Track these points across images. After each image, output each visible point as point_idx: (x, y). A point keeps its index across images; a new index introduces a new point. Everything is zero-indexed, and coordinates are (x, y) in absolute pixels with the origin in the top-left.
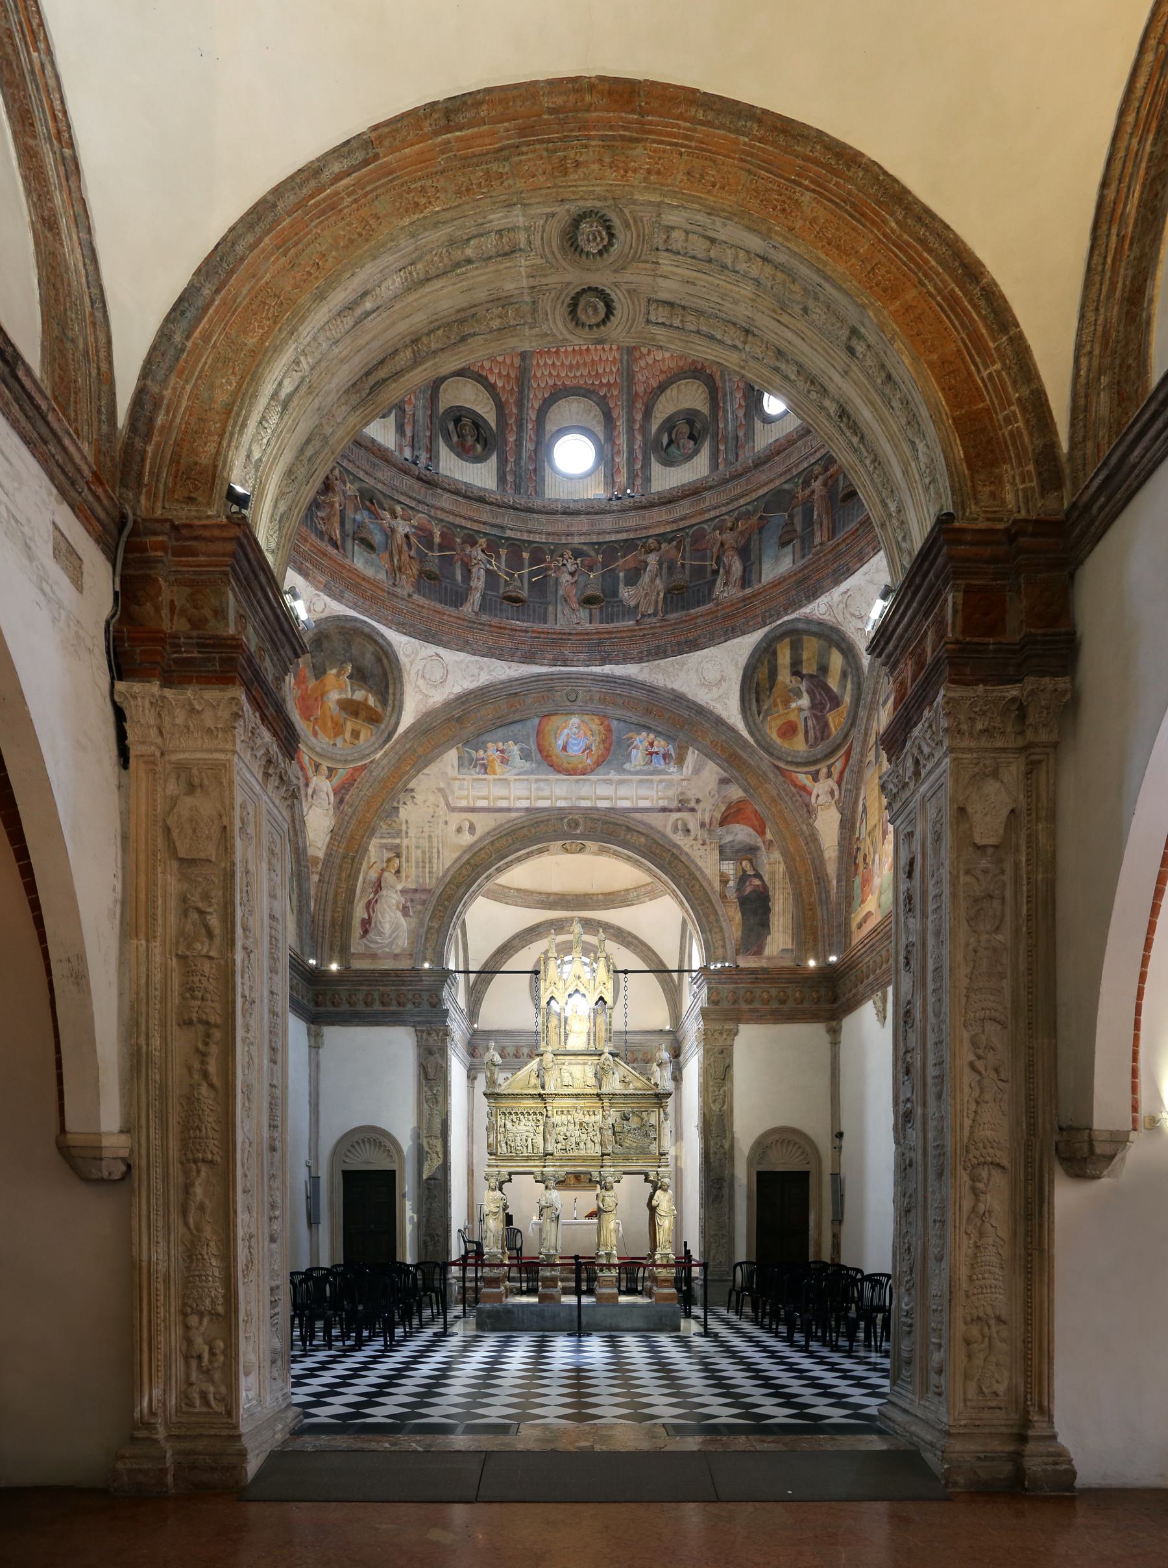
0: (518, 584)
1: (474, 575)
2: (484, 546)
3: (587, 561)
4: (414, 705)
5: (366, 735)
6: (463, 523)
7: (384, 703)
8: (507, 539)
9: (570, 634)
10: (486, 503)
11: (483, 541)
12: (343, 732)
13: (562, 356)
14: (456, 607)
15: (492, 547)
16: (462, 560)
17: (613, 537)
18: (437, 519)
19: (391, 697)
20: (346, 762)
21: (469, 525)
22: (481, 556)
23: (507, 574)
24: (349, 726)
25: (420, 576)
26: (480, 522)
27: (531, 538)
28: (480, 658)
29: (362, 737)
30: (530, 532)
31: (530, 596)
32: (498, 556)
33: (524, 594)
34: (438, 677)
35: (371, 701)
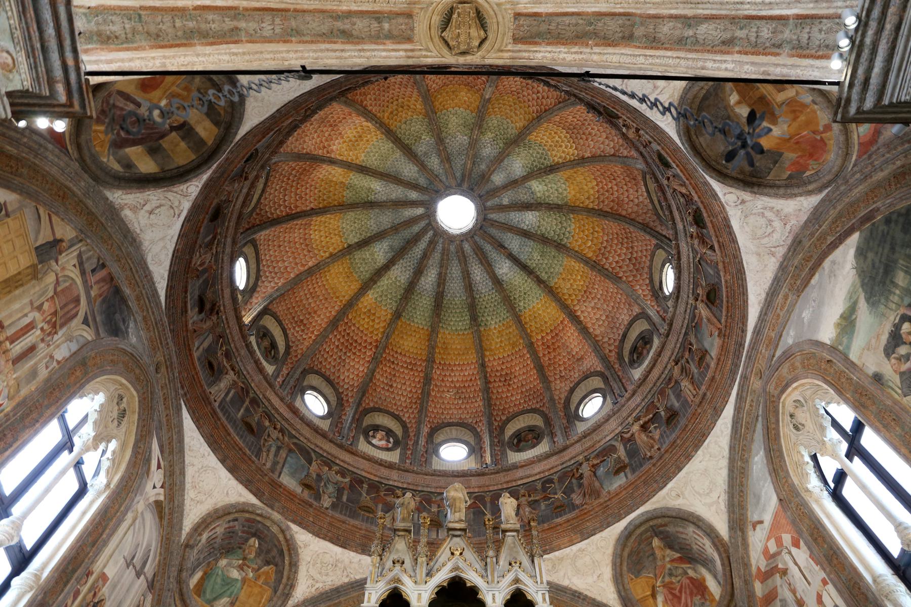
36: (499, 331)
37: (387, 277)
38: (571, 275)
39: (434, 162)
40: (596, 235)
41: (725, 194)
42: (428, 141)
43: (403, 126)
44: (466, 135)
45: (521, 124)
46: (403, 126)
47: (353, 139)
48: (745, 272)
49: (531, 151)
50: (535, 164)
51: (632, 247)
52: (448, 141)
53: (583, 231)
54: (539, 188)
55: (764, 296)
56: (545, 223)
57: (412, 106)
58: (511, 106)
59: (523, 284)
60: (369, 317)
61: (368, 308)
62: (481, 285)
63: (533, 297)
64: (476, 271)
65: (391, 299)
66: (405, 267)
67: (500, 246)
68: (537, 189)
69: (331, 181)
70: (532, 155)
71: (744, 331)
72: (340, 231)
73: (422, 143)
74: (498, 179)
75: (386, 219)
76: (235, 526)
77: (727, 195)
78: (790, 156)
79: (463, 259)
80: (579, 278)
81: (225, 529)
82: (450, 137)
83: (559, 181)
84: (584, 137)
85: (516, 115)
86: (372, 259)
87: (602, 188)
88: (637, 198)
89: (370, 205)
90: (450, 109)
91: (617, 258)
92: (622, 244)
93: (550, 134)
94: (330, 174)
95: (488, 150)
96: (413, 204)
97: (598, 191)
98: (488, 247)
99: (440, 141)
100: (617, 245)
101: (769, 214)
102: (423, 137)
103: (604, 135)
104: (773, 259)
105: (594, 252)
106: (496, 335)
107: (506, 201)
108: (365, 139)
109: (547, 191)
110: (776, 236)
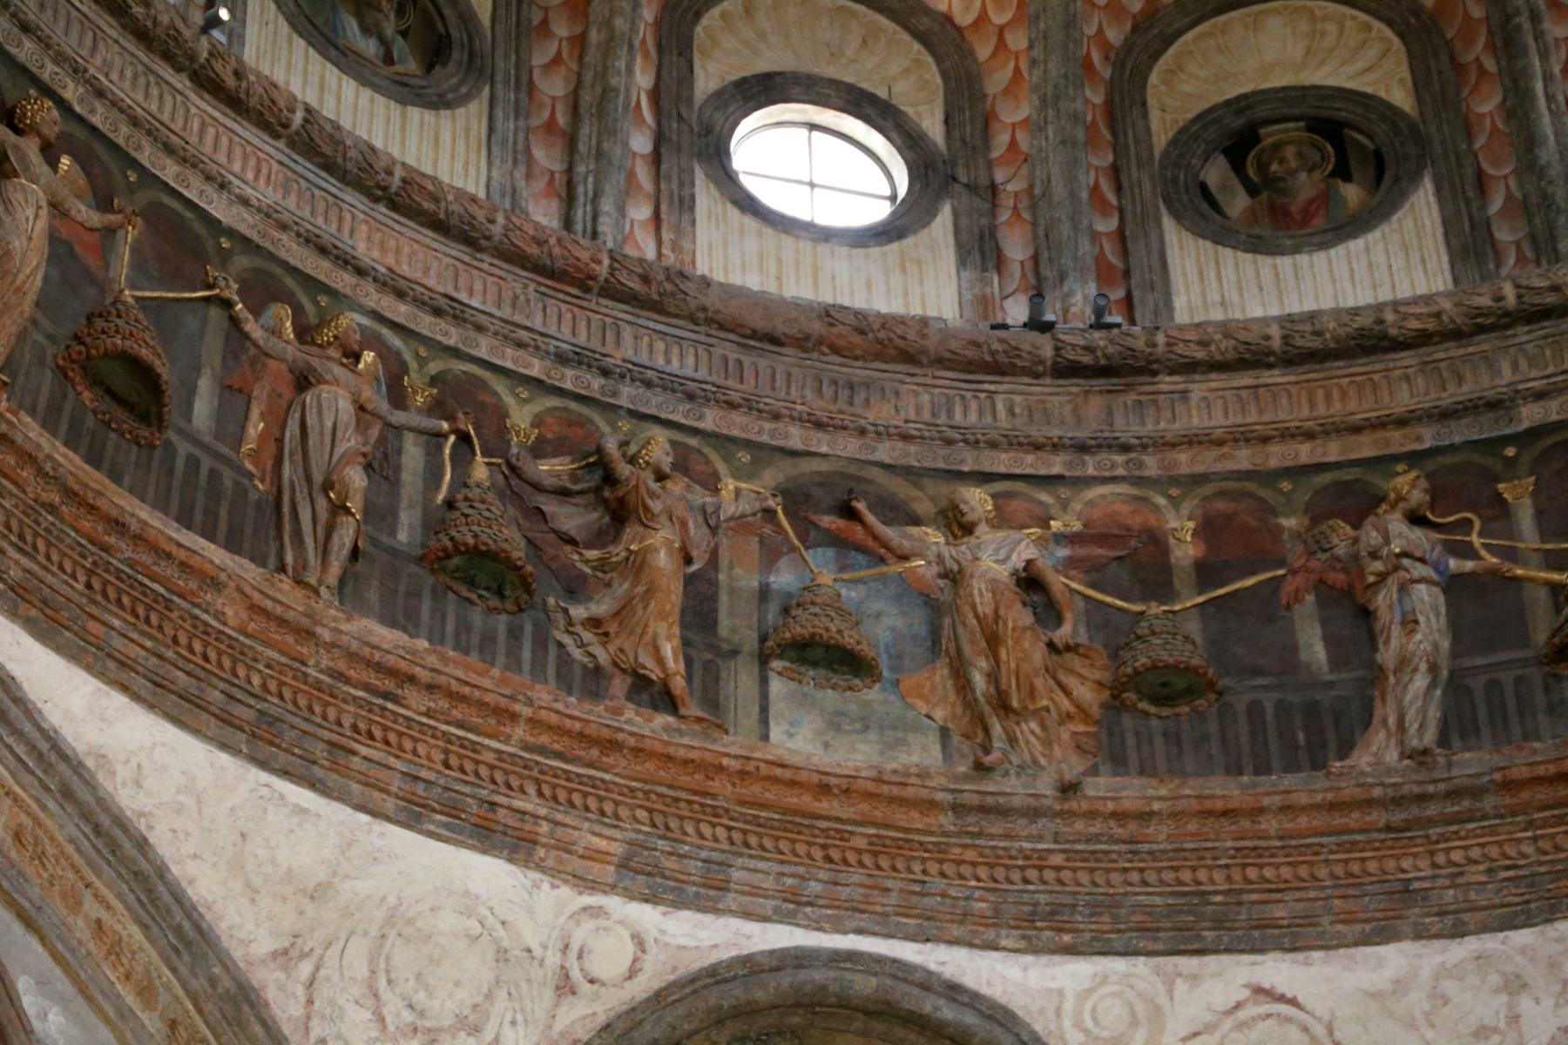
1: (1384, 616)
2: (1418, 496)
6: (1304, 453)
8: (1535, 433)
10: (1398, 345)
11: (1409, 485)
14: (1318, 764)
16: (1321, 586)
18: (1175, 480)
21: (1333, 451)
22: (1402, 535)
25: (1116, 702)
26: (1380, 424)
28: (1490, 943)
32: (1499, 511)
41: (640, 942)
48: (263, 765)
55: (127, 799)
77: (630, 948)
104: (264, 945)
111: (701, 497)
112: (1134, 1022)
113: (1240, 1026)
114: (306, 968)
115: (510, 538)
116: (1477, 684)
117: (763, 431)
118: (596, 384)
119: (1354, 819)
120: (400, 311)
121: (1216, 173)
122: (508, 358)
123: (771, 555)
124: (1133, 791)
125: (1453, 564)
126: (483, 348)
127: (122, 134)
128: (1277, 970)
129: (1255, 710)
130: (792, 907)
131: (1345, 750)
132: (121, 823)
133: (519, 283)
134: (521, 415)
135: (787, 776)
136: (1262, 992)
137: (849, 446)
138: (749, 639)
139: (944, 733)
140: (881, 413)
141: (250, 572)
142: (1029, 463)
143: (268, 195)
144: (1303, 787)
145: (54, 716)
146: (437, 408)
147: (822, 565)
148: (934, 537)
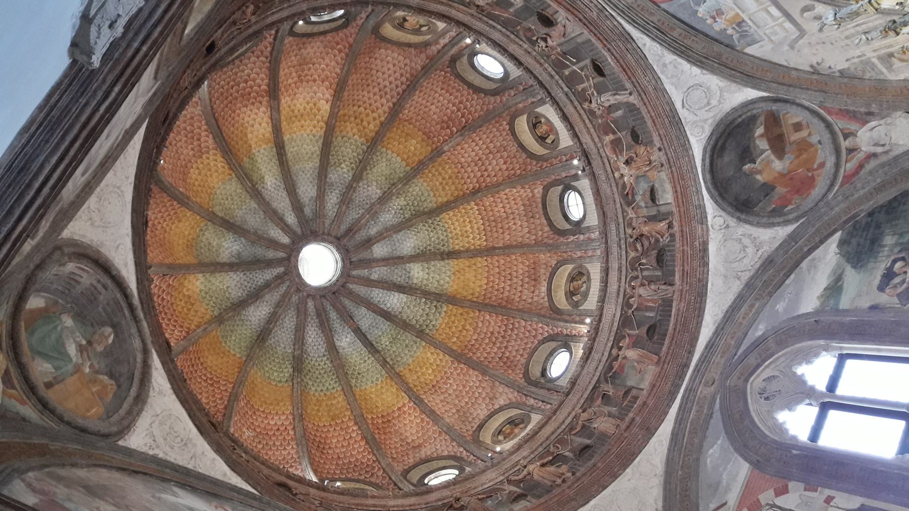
0: (585, 69)
3: (529, 34)
4: (736, 95)
5: (793, 116)
7: (753, 119)
8: (568, 87)
9: (580, 20)
12: (804, 140)
13: (459, 99)
15: (583, 97)
17: (499, 27)
19: (744, 117)
20: (828, 126)
23: (588, 80)
24: (795, 137)
27: (553, 73)
28: (658, 72)
29: (796, 120)
30: (552, 76)
31: (586, 58)
32: (584, 90)
33: (587, 62)
34: (699, 92)
35: (760, 131)
36: (318, 400)
37: (220, 279)
38: (421, 367)
39: (332, 199)
40: (464, 332)
41: (715, 217)
42: (344, 173)
43: (339, 138)
44: (381, 189)
45: (445, 199)
46: (339, 138)
47: (296, 112)
48: (706, 293)
49: (432, 234)
50: (429, 248)
51: (506, 347)
52: (361, 184)
53: (450, 328)
54: (418, 273)
55: (721, 316)
56: (409, 311)
57: (365, 123)
58: (444, 179)
59: (360, 364)
60: (186, 302)
61: (190, 293)
62: (311, 348)
63: (367, 380)
64: (310, 333)
65: (214, 303)
66: (242, 284)
67: (348, 318)
68: (416, 275)
69: (246, 135)
70: (430, 238)
71: (691, 353)
72: (211, 193)
73: (337, 171)
74: (379, 250)
75: (254, 219)
76: (100, 294)
77: (717, 218)
78: (780, 190)
79: (302, 313)
80: (430, 371)
81: (92, 284)
82: (365, 182)
83: (445, 273)
84: (501, 231)
85: (444, 189)
86: (217, 251)
87: (492, 287)
88: (532, 298)
89: (255, 192)
90: (389, 152)
91: (486, 355)
92: (494, 344)
93: (464, 221)
94: (253, 126)
95: (387, 217)
96: (286, 228)
97: (485, 290)
98: (333, 315)
99: (358, 177)
100: (487, 344)
101: (746, 241)
102: (343, 165)
103: (527, 230)
104: (738, 283)
105: (460, 347)
106: (314, 402)
107: (374, 276)
108: (303, 122)
109: (427, 279)
110: (746, 261)
111: (634, 221)
112: (697, 126)
113: (691, 107)
114: (740, 274)
115: (654, 253)
116: (614, 86)
117: (620, 211)
118: (623, 242)
119: (646, 100)
120: (623, 278)
121: (549, 141)
122: (624, 257)
123: (640, 207)
124: (656, 139)
125: (596, 95)
126: (624, 262)
127: (613, 334)
128: (678, 105)
129: (634, 120)
130: (699, 192)
131: (634, 105)
132: (724, 317)
133: (611, 258)
134: (632, 254)
135: (676, 198)
136: (683, 107)
137: (616, 196)
138: (655, 208)
139: (659, 172)
140: (608, 191)
141: (674, 304)
142: (607, 165)
143: (613, 306)
144: (644, 111)
145: (710, 334)
146: (636, 269)
147: (638, 198)
148: (626, 179)
